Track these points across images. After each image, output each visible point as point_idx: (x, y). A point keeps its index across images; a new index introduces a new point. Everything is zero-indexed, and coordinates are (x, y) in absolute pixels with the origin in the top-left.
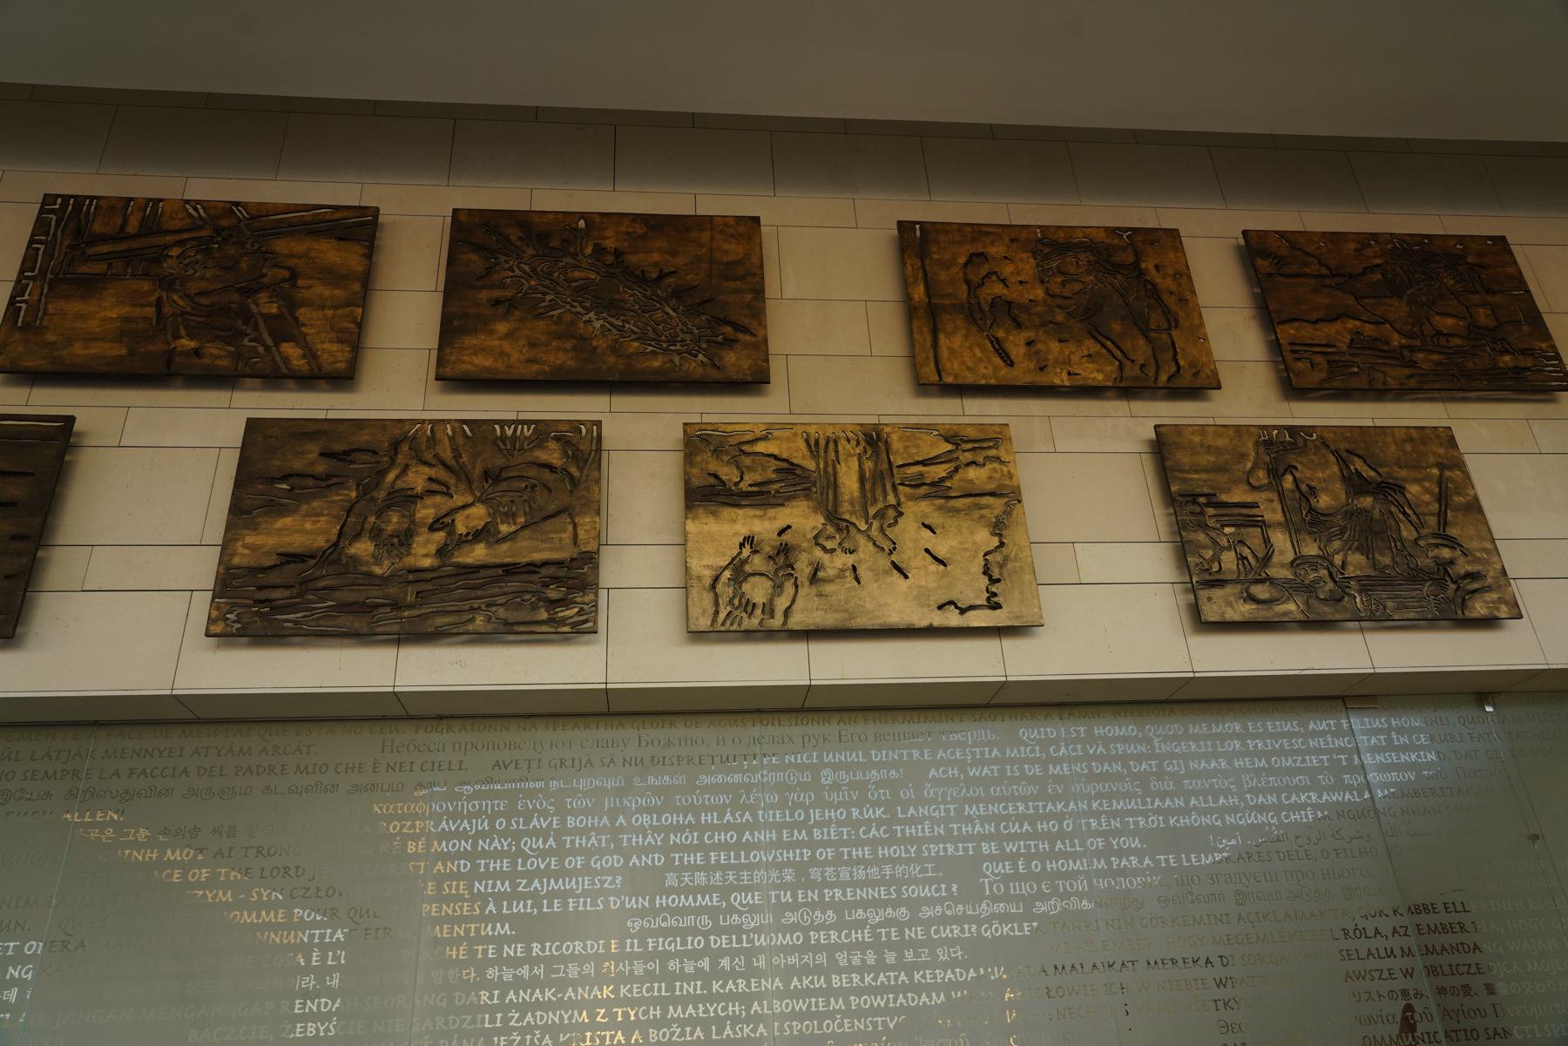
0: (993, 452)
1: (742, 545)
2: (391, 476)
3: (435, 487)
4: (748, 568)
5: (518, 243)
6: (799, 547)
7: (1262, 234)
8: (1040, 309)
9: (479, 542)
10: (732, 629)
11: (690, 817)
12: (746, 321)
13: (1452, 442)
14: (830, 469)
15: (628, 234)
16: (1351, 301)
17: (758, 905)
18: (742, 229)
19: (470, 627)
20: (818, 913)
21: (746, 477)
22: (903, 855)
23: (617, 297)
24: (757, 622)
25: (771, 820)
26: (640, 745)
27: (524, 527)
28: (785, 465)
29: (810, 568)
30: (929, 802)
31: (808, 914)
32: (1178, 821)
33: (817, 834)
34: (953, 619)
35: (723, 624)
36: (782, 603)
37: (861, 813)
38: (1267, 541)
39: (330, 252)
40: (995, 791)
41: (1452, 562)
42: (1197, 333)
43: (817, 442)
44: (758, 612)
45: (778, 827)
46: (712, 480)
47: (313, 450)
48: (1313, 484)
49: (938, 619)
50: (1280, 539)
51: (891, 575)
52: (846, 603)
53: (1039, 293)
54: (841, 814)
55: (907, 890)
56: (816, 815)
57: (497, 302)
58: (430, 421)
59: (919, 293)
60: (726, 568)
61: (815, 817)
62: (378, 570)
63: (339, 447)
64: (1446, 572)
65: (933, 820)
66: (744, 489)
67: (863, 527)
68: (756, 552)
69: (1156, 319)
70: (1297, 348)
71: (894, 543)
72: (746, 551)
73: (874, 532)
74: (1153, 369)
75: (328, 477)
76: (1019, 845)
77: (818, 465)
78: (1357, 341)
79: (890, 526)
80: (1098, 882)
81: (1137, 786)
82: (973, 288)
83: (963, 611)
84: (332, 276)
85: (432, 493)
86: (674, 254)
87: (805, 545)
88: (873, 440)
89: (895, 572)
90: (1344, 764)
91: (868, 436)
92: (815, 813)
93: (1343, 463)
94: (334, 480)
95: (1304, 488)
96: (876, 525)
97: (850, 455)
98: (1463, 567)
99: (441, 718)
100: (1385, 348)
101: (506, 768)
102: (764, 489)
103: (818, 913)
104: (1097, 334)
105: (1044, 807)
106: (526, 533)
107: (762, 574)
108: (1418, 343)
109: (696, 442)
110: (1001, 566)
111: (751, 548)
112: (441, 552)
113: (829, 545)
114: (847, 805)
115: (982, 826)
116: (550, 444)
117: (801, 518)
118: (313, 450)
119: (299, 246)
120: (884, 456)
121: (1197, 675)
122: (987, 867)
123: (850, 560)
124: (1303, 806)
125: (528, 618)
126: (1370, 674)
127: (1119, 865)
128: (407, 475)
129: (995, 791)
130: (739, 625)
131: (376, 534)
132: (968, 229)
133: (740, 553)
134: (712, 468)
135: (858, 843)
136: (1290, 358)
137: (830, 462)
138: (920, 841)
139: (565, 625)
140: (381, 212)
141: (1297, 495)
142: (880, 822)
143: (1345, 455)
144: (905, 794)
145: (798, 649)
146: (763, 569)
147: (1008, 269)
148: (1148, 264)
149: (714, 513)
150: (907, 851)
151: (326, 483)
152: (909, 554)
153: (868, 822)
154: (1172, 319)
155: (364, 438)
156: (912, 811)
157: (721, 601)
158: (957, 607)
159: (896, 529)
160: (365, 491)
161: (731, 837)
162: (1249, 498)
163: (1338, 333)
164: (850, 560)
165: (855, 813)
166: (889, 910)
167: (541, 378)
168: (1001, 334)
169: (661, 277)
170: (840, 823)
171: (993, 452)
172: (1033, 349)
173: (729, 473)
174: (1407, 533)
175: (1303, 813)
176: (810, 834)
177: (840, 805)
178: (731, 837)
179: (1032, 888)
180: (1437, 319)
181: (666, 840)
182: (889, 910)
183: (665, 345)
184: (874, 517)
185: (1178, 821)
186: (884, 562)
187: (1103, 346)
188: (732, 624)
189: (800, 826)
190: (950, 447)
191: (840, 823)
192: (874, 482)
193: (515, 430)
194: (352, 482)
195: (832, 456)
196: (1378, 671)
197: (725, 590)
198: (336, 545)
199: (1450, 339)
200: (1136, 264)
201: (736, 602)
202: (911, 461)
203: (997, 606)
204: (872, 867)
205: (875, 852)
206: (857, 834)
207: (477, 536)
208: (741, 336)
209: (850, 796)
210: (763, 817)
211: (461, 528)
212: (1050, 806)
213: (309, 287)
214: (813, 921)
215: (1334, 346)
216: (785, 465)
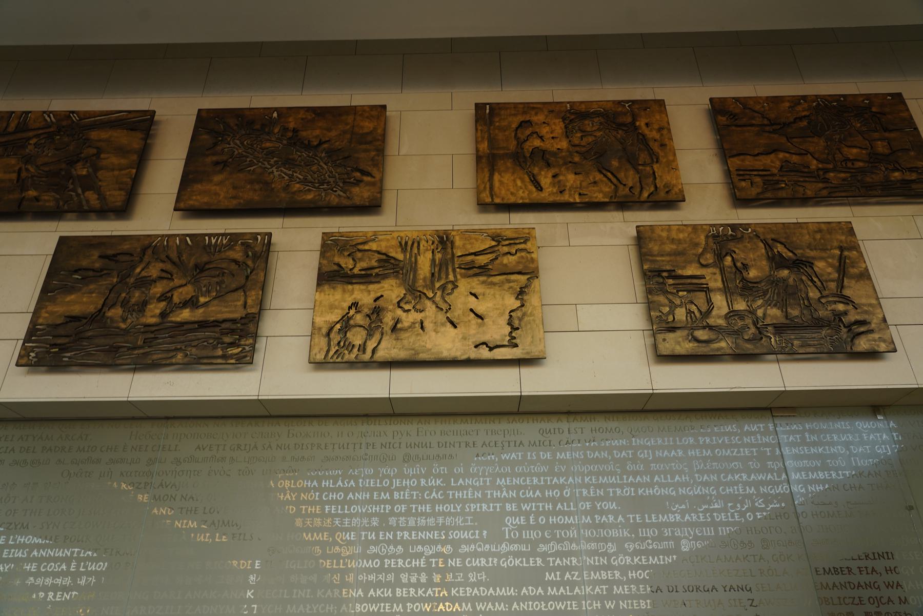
0: (522, 246)
1: (350, 308)
2: (138, 270)
3: (164, 275)
4: (352, 322)
5: (235, 128)
6: (387, 308)
7: (723, 100)
8: (564, 154)
9: (186, 308)
10: (337, 360)
11: (315, 483)
12: (369, 169)
13: (851, 232)
14: (413, 259)
15: (302, 119)
16: (784, 140)
17: (325, 541)
18: (374, 113)
19: (174, 361)
20: (392, 547)
21: (358, 265)
22: (452, 510)
23: (291, 157)
24: (354, 356)
25: (367, 485)
26: (288, 437)
27: (215, 298)
28: (384, 257)
29: (392, 322)
30: (473, 476)
31: (385, 548)
32: (644, 491)
33: (396, 495)
34: (485, 353)
35: (332, 358)
36: (371, 345)
37: (427, 483)
38: (709, 301)
39: (122, 137)
40: (518, 469)
41: (845, 313)
42: (672, 166)
43: (406, 243)
44: (355, 350)
45: (371, 490)
46: (336, 268)
47: (96, 254)
48: (745, 262)
49: (473, 354)
50: (719, 300)
51: (446, 326)
52: (413, 344)
53: (564, 144)
54: (413, 482)
55: (452, 534)
56: (397, 483)
57: (217, 163)
58: (167, 235)
59: (484, 146)
60: (338, 322)
61: (396, 484)
62: (123, 326)
63: (110, 252)
64: (841, 320)
65: (474, 488)
66: (355, 273)
67: (430, 295)
68: (358, 312)
69: (643, 157)
70: (741, 173)
71: (450, 306)
72: (352, 312)
73: (438, 298)
74: (638, 190)
75: (102, 270)
76: (532, 506)
77: (405, 256)
78: (786, 168)
79: (448, 294)
80: (584, 532)
81: (618, 468)
83: (491, 349)
84: (121, 151)
85: (161, 278)
86: (329, 130)
87: (391, 307)
88: (444, 240)
89: (449, 324)
90: (768, 454)
91: (441, 238)
92: (396, 481)
94: (105, 272)
95: (739, 264)
96: (439, 293)
97: (427, 250)
98: (853, 317)
99: (167, 418)
100: (806, 170)
101: (204, 449)
102: (369, 272)
103: (392, 547)
104: (602, 169)
105: (551, 481)
106: (216, 302)
107: (361, 326)
108: (831, 166)
109: (330, 244)
110: (520, 319)
111: (356, 309)
112: (163, 315)
113: (407, 307)
114: (418, 477)
115: (508, 492)
116: (237, 247)
117: (392, 290)
118: (96, 254)
119: (104, 135)
120: (449, 250)
121: (655, 391)
122: (509, 520)
123: (418, 316)
124: (736, 483)
125: (210, 354)
126: (783, 392)
127: (600, 521)
128: (148, 268)
129: (518, 469)
130: (342, 358)
131: (125, 304)
132: (521, 106)
133: (348, 313)
134: (336, 259)
135: (423, 502)
136: (736, 179)
137: (414, 255)
138: (464, 501)
139: (232, 359)
140: (157, 114)
141: (734, 269)
142: (438, 488)
143: (770, 242)
144: (457, 470)
145: (384, 374)
146: (361, 323)
147: (544, 131)
148: (641, 123)
149: (334, 288)
150: (455, 508)
151: (99, 274)
153: (431, 489)
154: (654, 157)
155: (126, 247)
156: (461, 481)
157: (332, 343)
158: (487, 346)
159: (452, 297)
160: (123, 279)
161: (340, 496)
162: (698, 272)
163: (772, 162)
164: (418, 316)
165: (423, 482)
166: (439, 547)
167: (239, 207)
168: (536, 170)
169: (320, 143)
170: (412, 489)
171: (522, 246)
172: (556, 180)
173: (347, 263)
174: (813, 294)
175: (736, 488)
176: (392, 495)
177: (414, 476)
178: (340, 496)
179: (538, 534)
180: (845, 150)
181: (298, 497)
182: (439, 547)
183: (317, 185)
184: (438, 289)
185: (644, 491)
186: (441, 317)
187: (605, 176)
188: (337, 358)
189: (385, 490)
190: (494, 243)
191: (412, 489)
192: (440, 268)
193: (217, 240)
194: (115, 273)
195: (415, 251)
196: (787, 389)
197: (335, 337)
198: (100, 311)
199: (855, 162)
200: (633, 123)
201: (342, 344)
202: (467, 253)
203: (516, 346)
204: (430, 517)
205: (433, 508)
206: (423, 496)
207: (185, 304)
208: (366, 179)
209: (420, 471)
210: (362, 484)
211: (176, 299)
212: (555, 480)
213: (107, 158)
214: (387, 552)
215: (769, 170)
216: (384, 257)
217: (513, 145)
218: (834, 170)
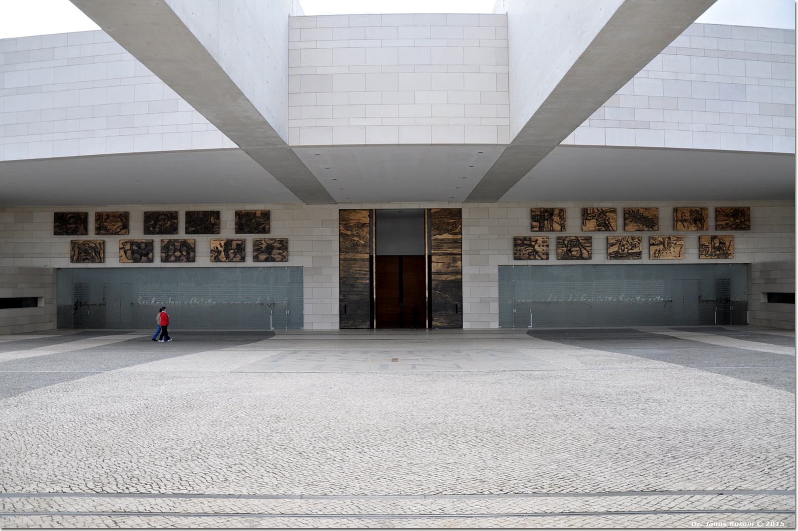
16: (727, 218)
39: (612, 214)
49: (674, 258)
57: (630, 221)
59: (676, 219)
69: (703, 221)
78: (726, 224)
82: (682, 217)
84: (613, 219)
93: (720, 240)
98: (729, 252)
104: (695, 223)
112: (628, 251)
117: (661, 247)
151: (616, 244)
152: (672, 251)
163: (723, 223)
186: (669, 252)
207: (630, 249)
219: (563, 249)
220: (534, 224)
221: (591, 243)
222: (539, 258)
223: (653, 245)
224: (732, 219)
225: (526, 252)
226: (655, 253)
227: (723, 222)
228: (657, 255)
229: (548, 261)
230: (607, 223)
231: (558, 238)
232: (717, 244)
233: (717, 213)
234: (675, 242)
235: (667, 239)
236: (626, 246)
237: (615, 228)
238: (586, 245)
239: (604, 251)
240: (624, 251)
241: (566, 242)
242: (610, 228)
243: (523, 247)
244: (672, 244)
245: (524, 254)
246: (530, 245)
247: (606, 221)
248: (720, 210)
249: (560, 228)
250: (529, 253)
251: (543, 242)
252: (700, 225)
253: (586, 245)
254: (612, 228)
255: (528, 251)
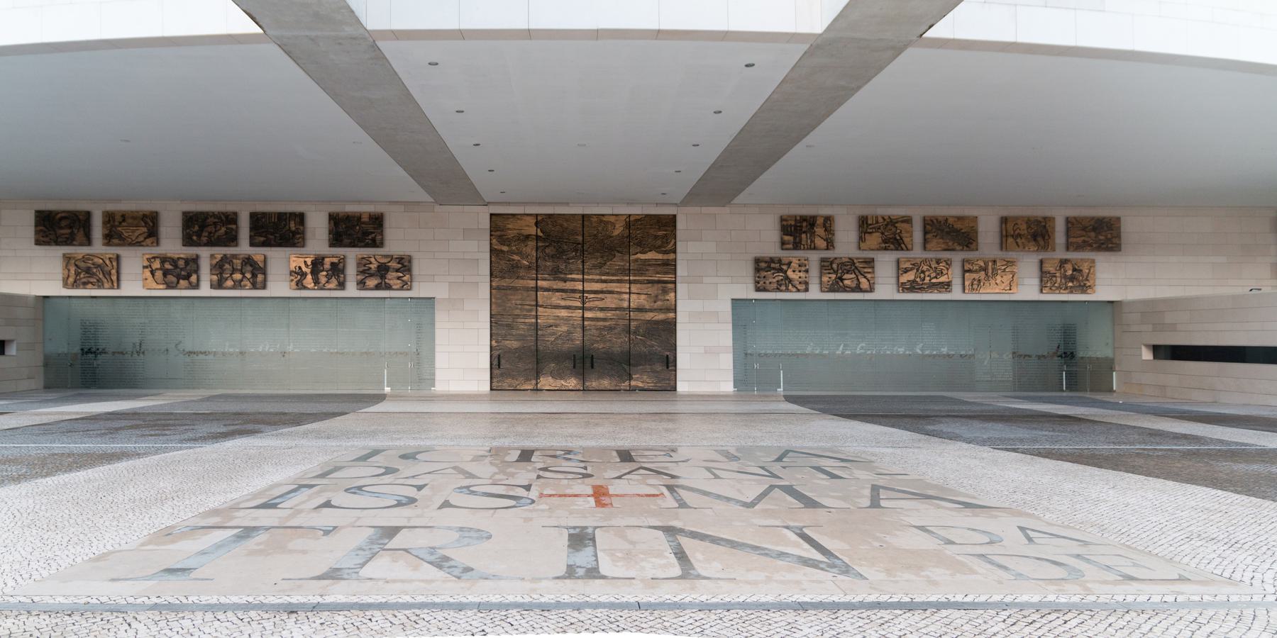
34: (1004, 291)
39: (905, 225)
49: (1001, 291)
53: (1026, 232)
59: (1004, 233)
69: (1047, 237)
104: (1035, 240)
148: (1047, 226)
151: (912, 269)
217: (1012, 233)
218: (1095, 243)
219: (830, 275)
220: (786, 238)
221: (873, 267)
222: (794, 290)
223: (969, 271)
224: (1093, 234)
225: (774, 280)
226: (972, 285)
227: (1078, 239)
228: (975, 287)
229: (807, 293)
230: (898, 238)
231: (823, 260)
232: (1070, 272)
233: (1070, 225)
234: (1003, 268)
235: (990, 264)
236: (927, 273)
237: (909, 246)
238: (866, 270)
239: (893, 280)
240: (924, 280)
241: (835, 266)
242: (903, 246)
243: (769, 273)
244: (999, 272)
245: (770, 283)
246: (781, 270)
247: (897, 236)
248: (1074, 221)
249: (826, 245)
250: (778, 281)
251: (800, 266)
252: (1042, 243)
253: (866, 270)
254: (906, 247)
255: (777, 279)
